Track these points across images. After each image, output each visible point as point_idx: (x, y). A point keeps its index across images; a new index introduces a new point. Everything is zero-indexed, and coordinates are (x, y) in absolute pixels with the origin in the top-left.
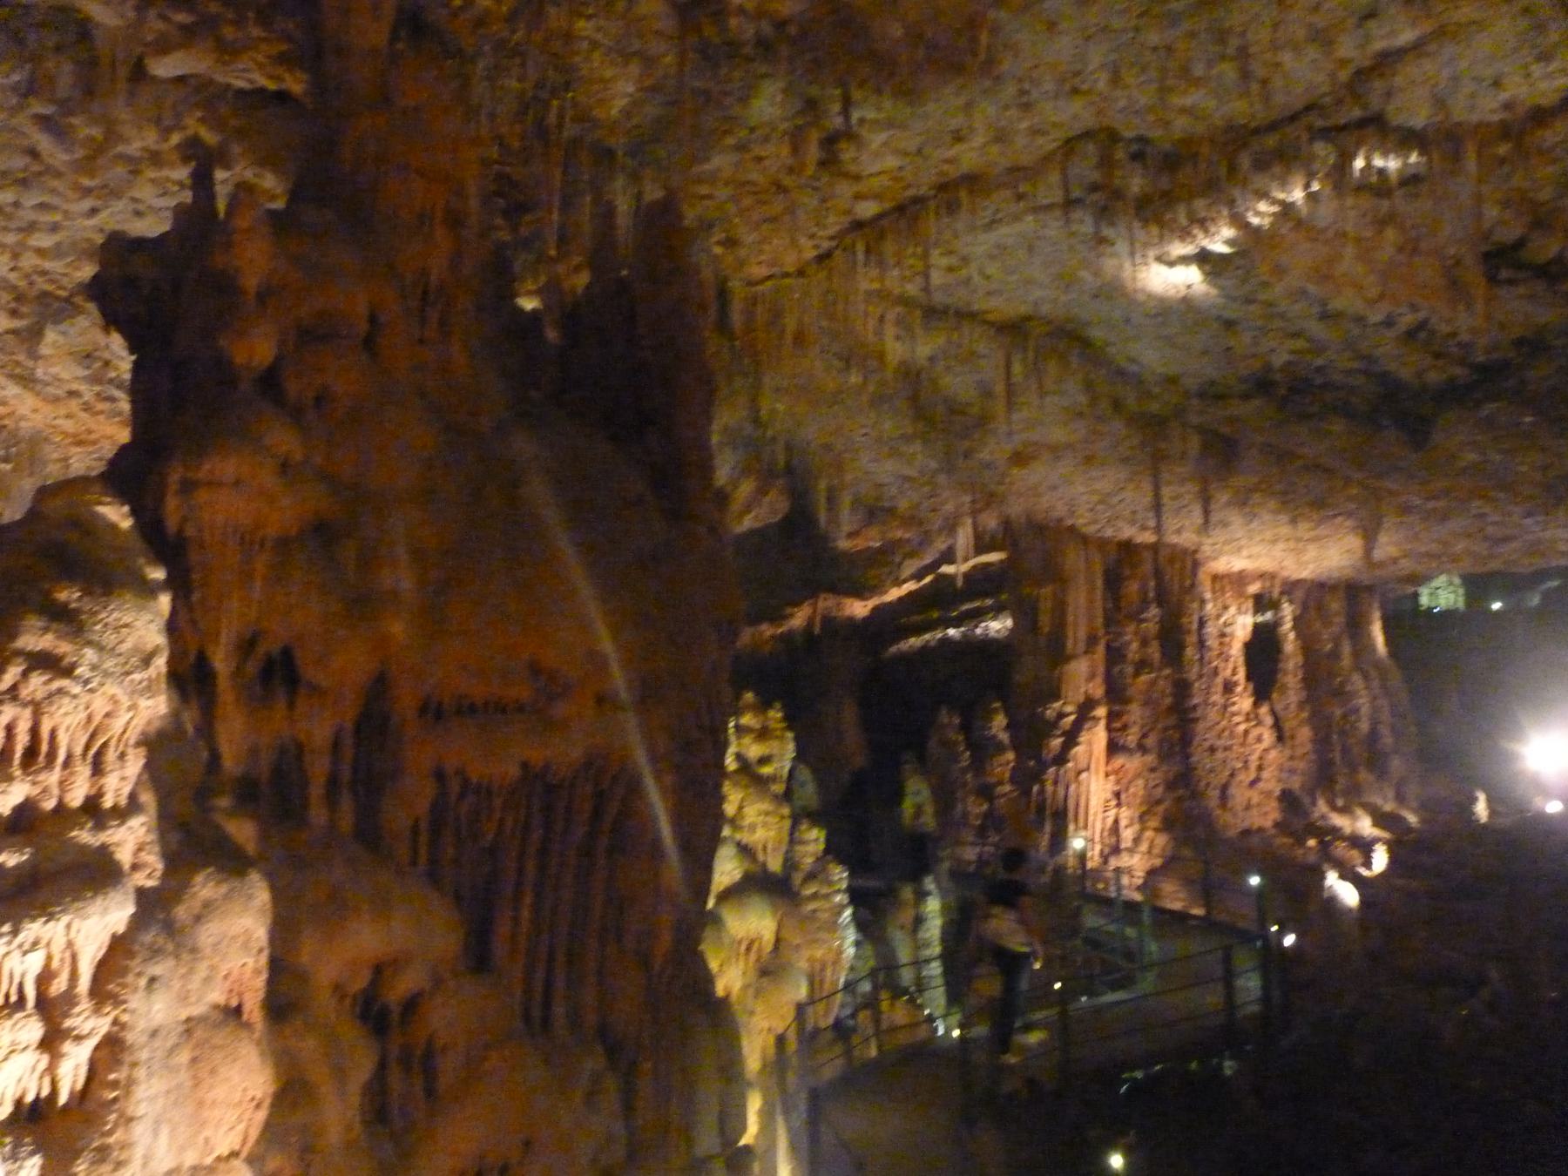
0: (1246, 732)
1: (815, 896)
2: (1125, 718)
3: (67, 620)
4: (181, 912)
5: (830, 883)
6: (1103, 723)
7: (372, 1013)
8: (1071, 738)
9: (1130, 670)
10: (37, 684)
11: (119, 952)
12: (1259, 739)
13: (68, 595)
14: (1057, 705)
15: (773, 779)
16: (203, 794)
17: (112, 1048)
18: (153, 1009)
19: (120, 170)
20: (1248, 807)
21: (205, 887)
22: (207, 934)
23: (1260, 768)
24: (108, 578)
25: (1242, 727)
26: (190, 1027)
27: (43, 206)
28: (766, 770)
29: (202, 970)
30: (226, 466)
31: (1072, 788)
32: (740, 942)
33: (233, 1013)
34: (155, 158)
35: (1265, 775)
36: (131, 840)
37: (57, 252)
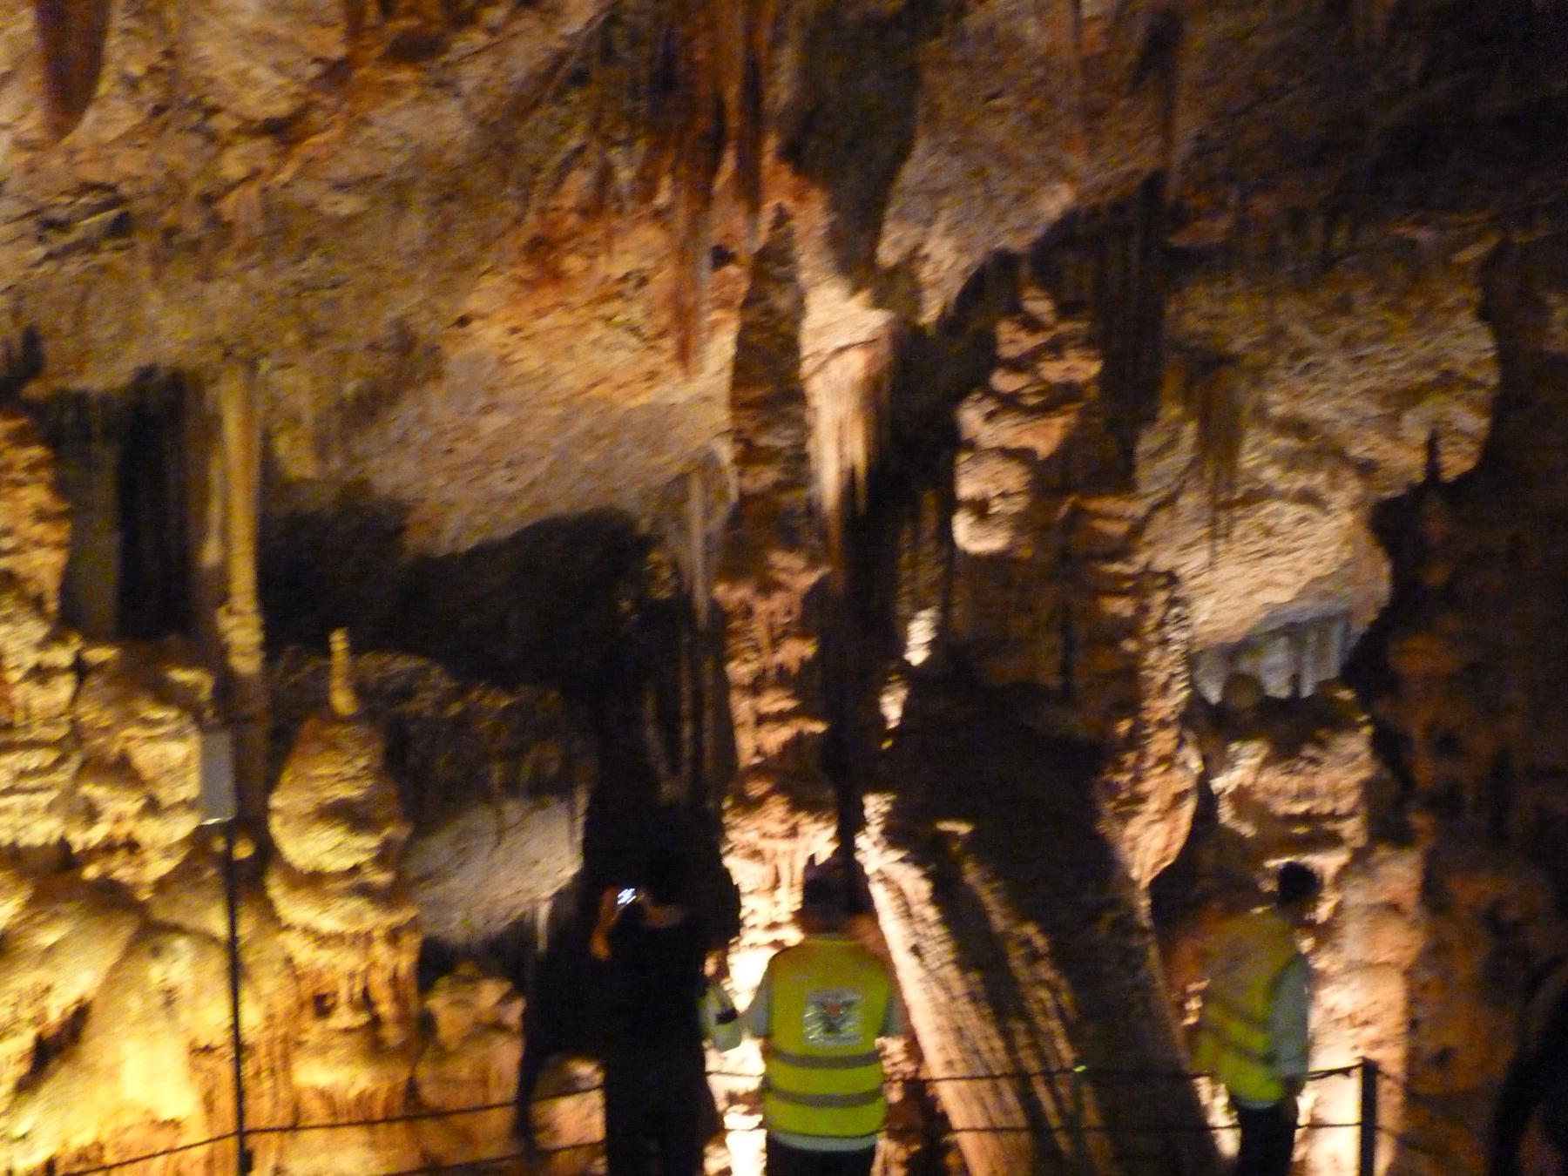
3: (1322, 744)
4: (1374, 859)
7: (1493, 920)
10: (1310, 769)
11: (1344, 871)
13: (1322, 733)
16: (1399, 806)
17: (1338, 909)
18: (1357, 896)
21: (1382, 852)
22: (1383, 870)
24: (1339, 722)
26: (1374, 906)
29: (1378, 887)
30: (1419, 643)
33: (1394, 908)
36: (1350, 828)
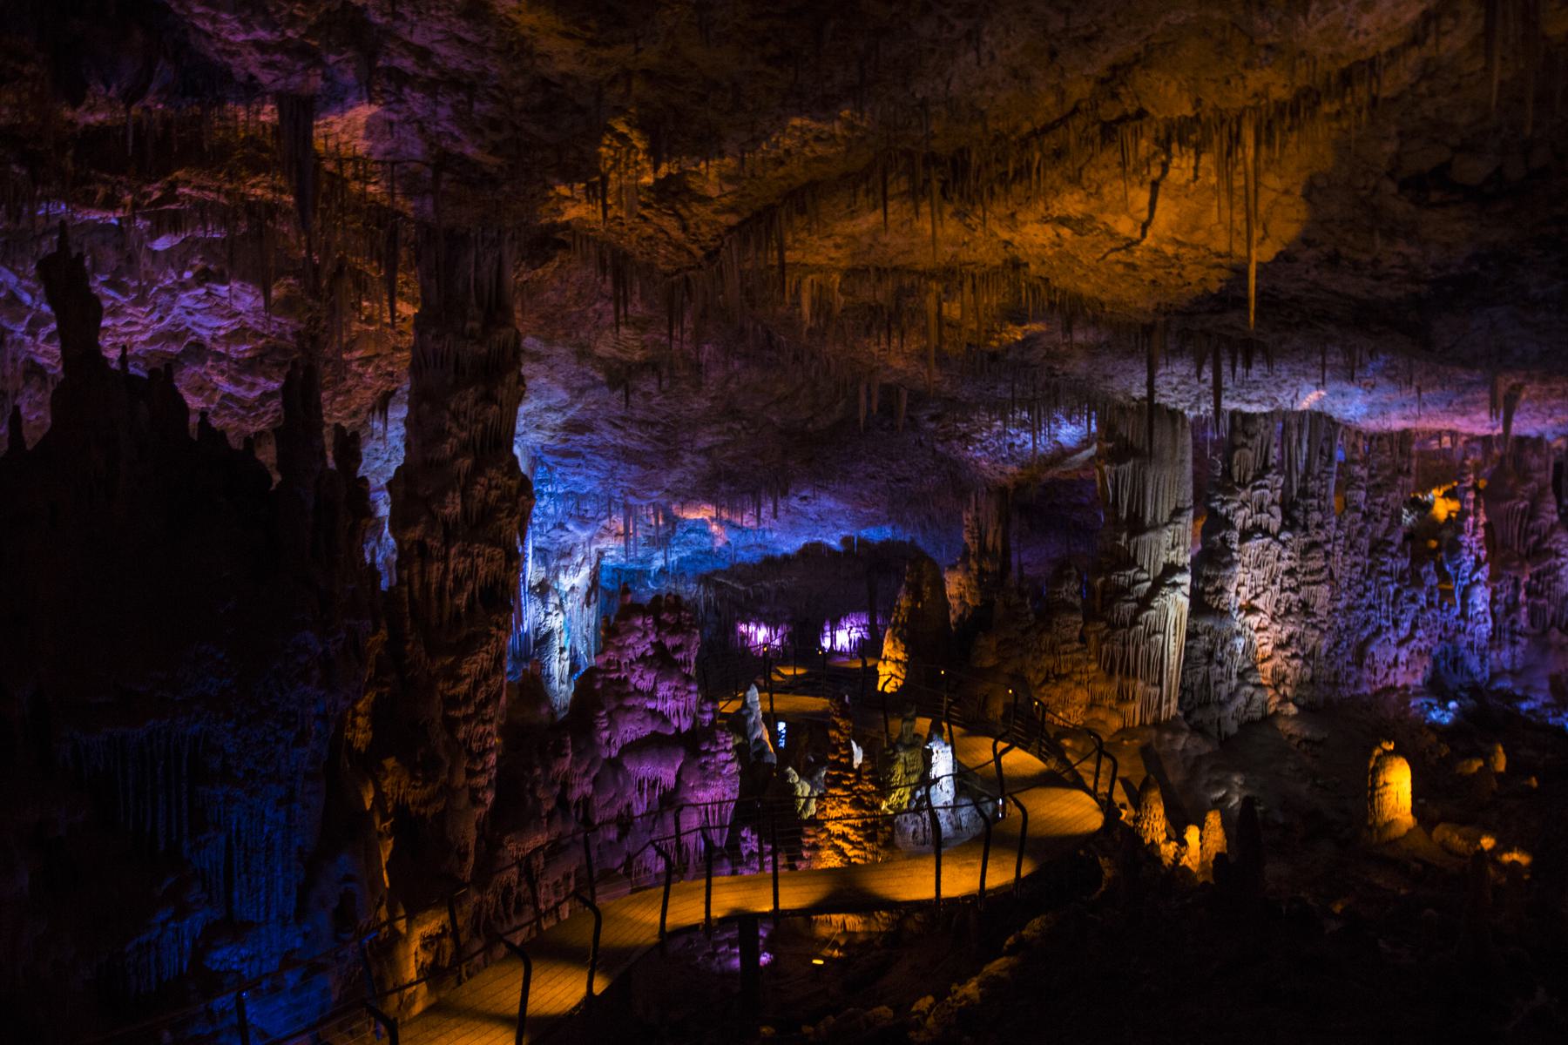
0: (1398, 592)
1: (707, 753)
2: (1218, 584)
5: (717, 744)
6: (1186, 589)
8: (1145, 603)
9: (1236, 535)
12: (1413, 599)
14: (1131, 573)
15: (685, 663)
19: (164, 298)
20: (1396, 662)
23: (1414, 626)
25: (1391, 589)
27: (129, 324)
28: (678, 656)
31: (1142, 648)
32: (641, 782)
34: (184, 287)
35: (1420, 633)
37: (152, 340)
